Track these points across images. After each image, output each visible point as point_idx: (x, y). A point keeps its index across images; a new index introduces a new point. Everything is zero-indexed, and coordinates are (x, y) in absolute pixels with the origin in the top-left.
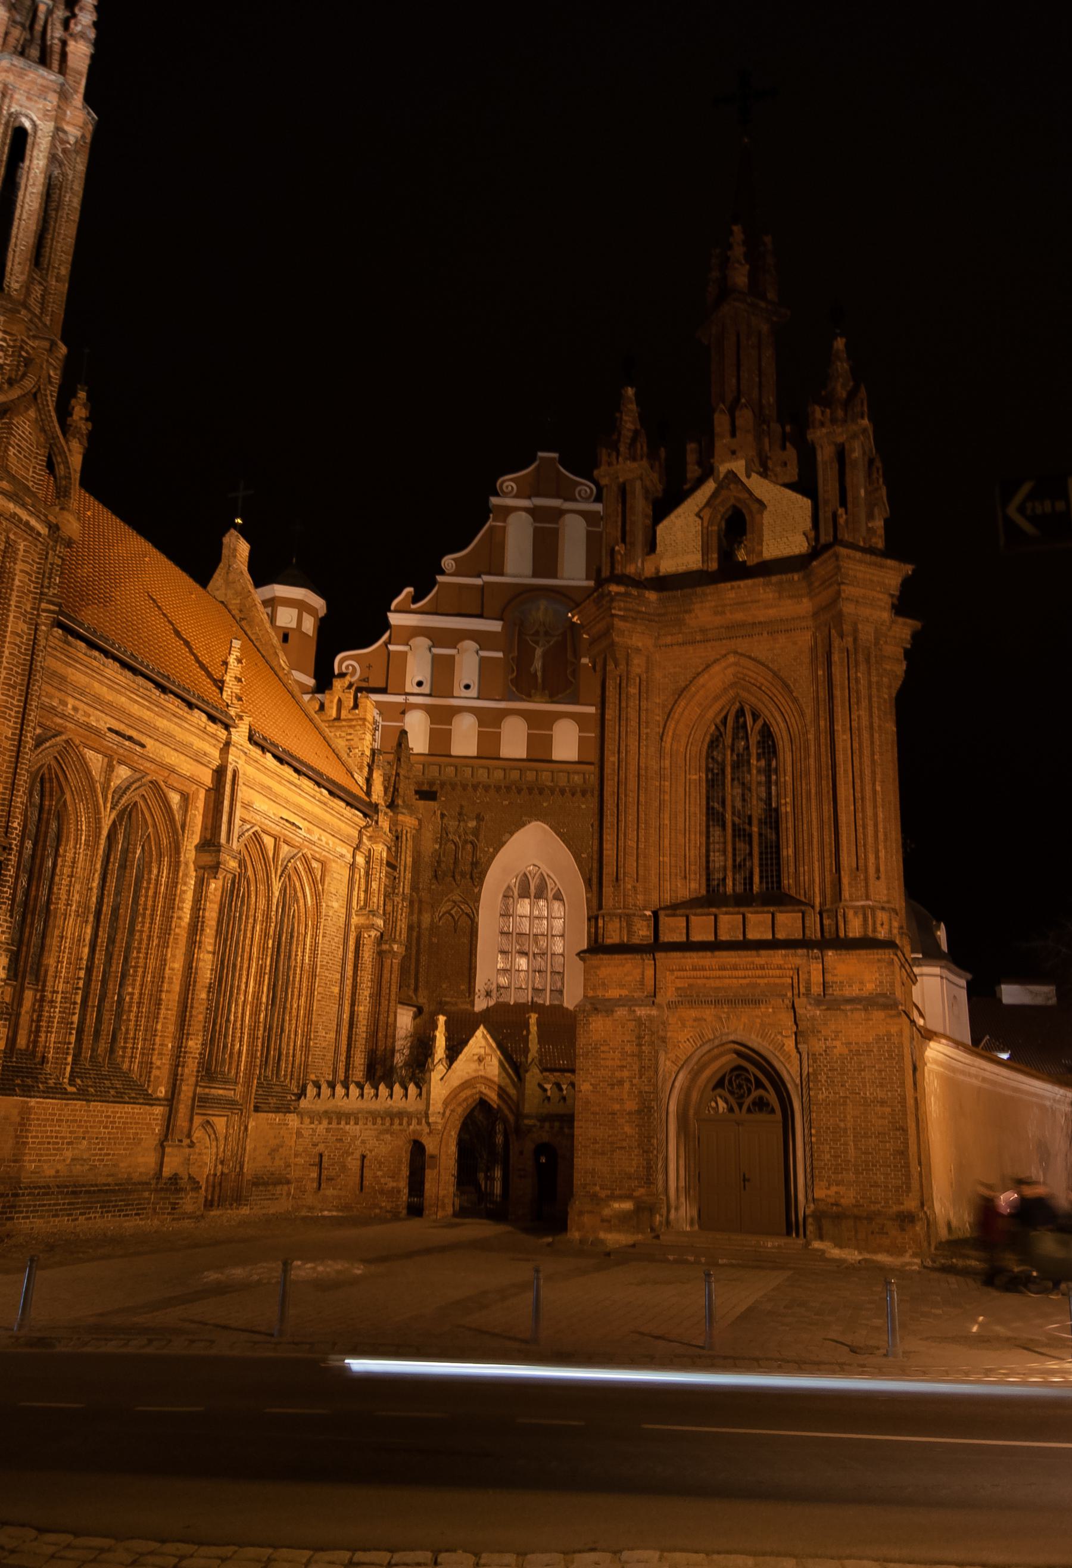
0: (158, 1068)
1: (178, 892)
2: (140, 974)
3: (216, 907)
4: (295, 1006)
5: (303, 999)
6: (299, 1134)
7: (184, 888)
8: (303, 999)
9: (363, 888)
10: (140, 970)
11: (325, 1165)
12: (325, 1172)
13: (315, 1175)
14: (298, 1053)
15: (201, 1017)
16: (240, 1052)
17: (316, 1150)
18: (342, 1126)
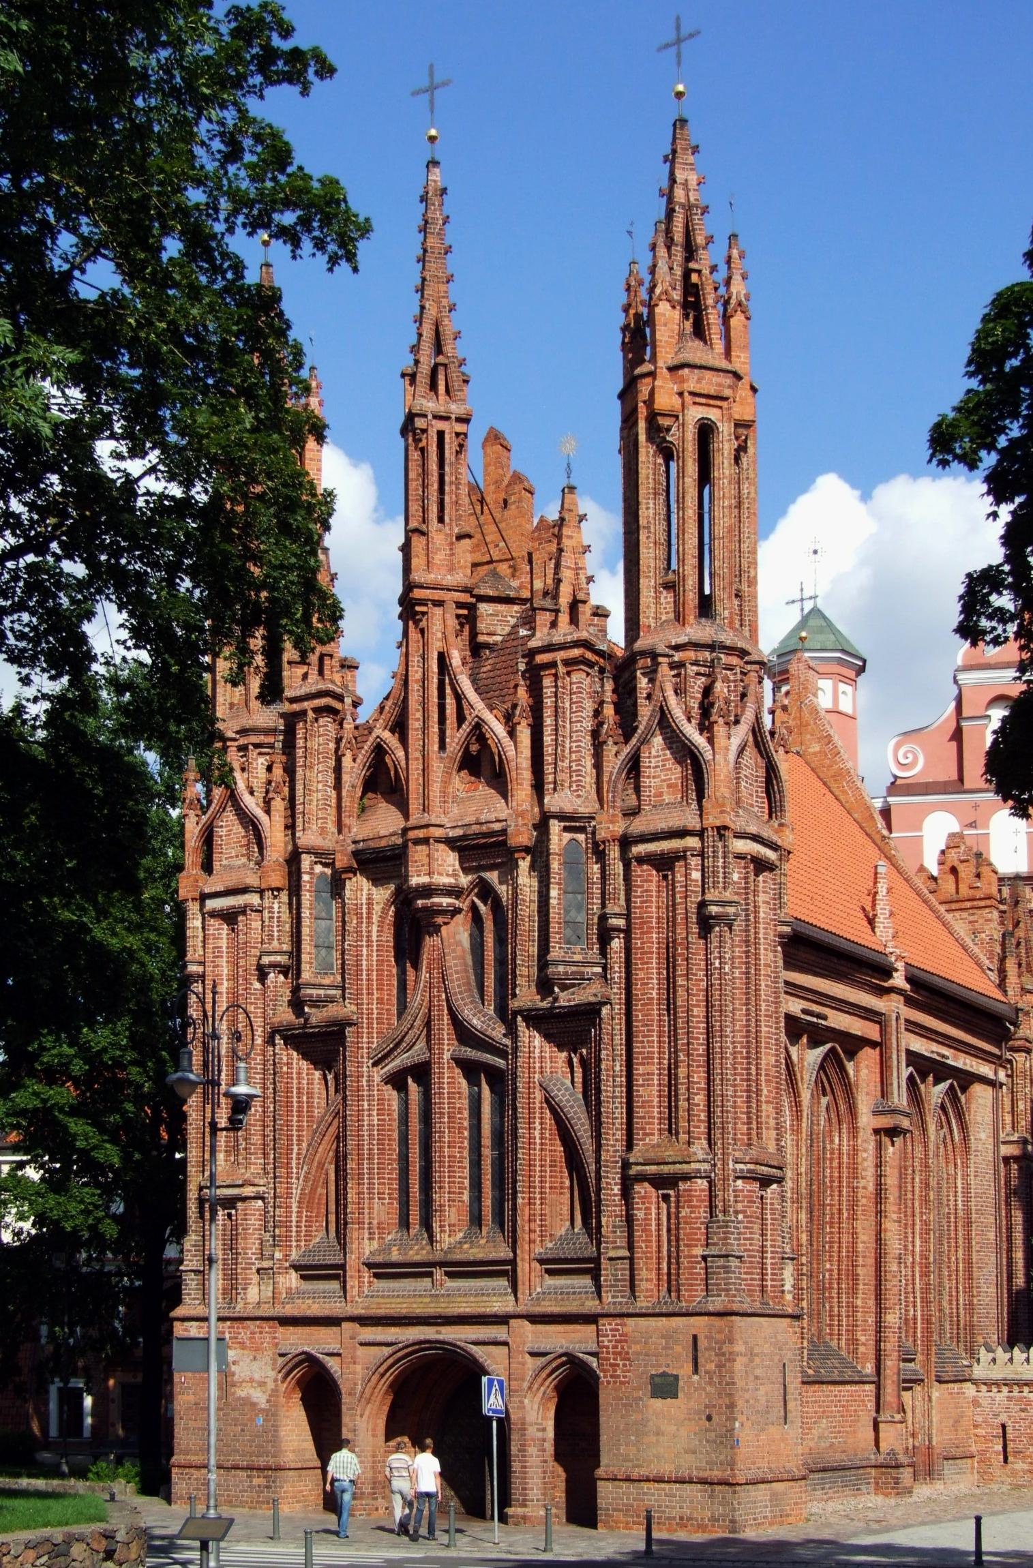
0: (864, 1344)
1: (860, 1160)
2: (836, 1249)
3: (896, 1172)
4: (953, 1259)
5: (961, 1252)
6: (976, 1403)
7: (865, 1155)
8: (961, 1252)
9: (1008, 1107)
10: (836, 1245)
11: (1010, 1436)
12: (1010, 1446)
13: (999, 1448)
14: (962, 1312)
15: (895, 1291)
16: (915, 1318)
17: (998, 1421)
18: (1025, 1394)
